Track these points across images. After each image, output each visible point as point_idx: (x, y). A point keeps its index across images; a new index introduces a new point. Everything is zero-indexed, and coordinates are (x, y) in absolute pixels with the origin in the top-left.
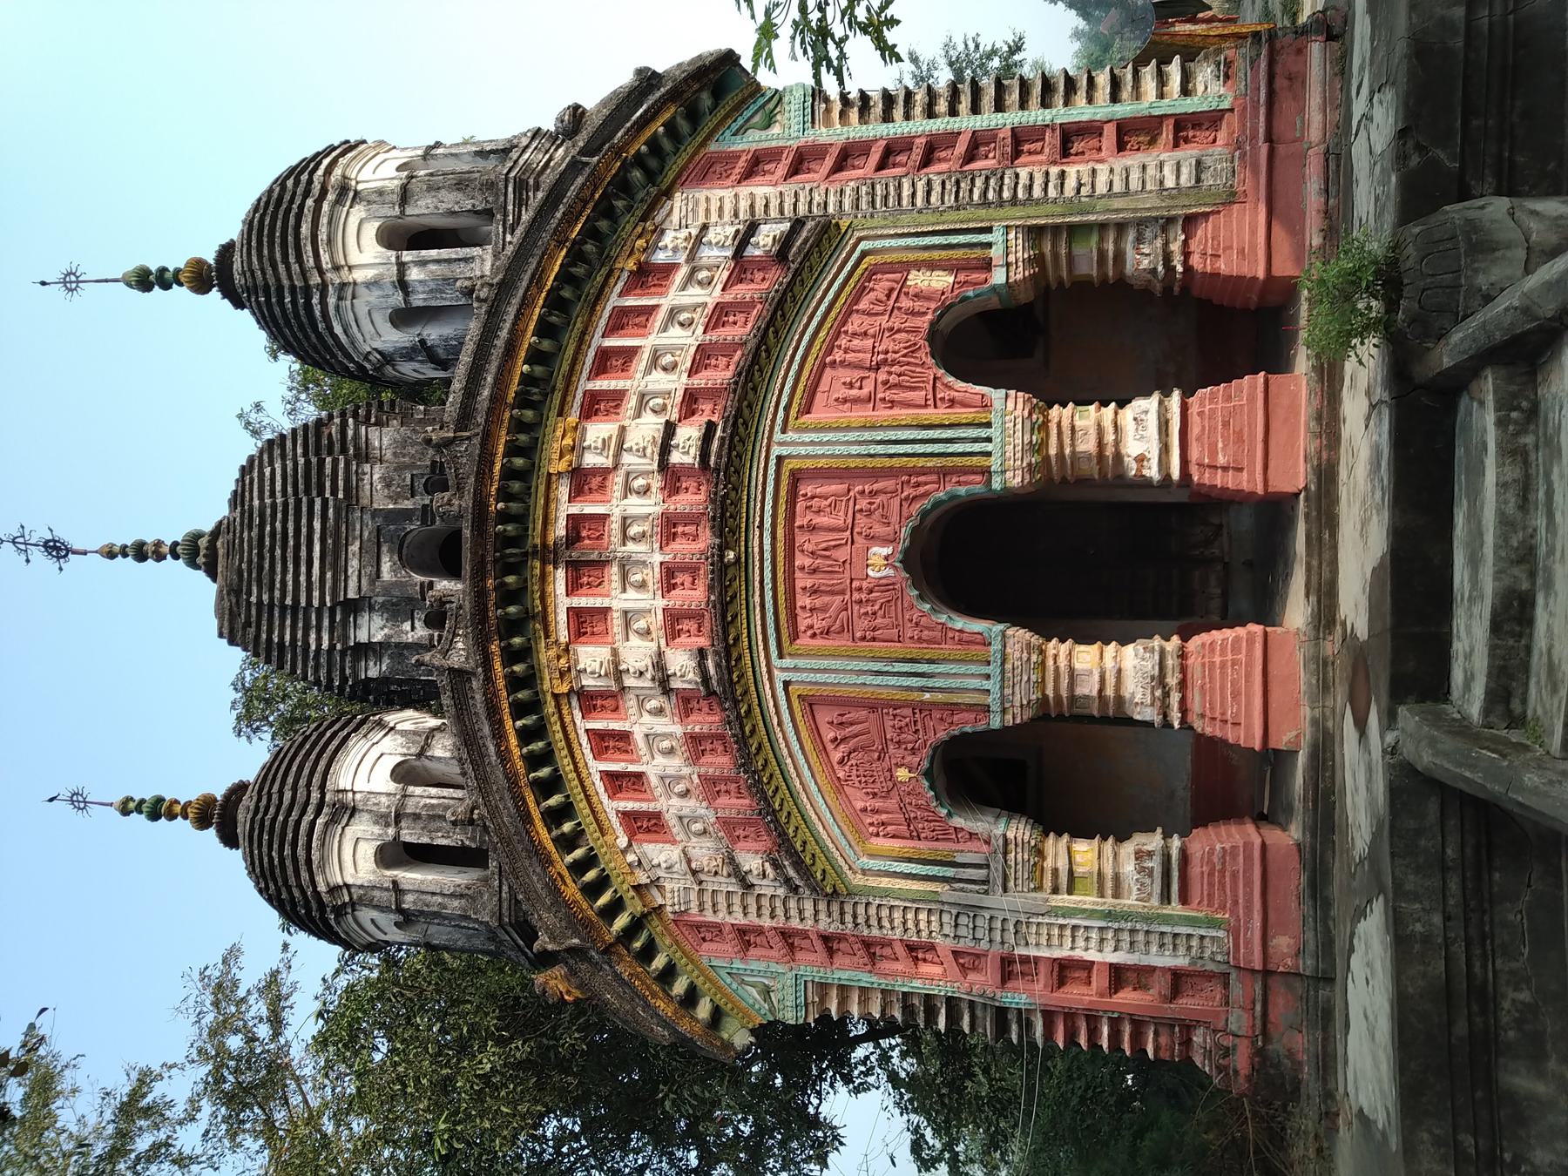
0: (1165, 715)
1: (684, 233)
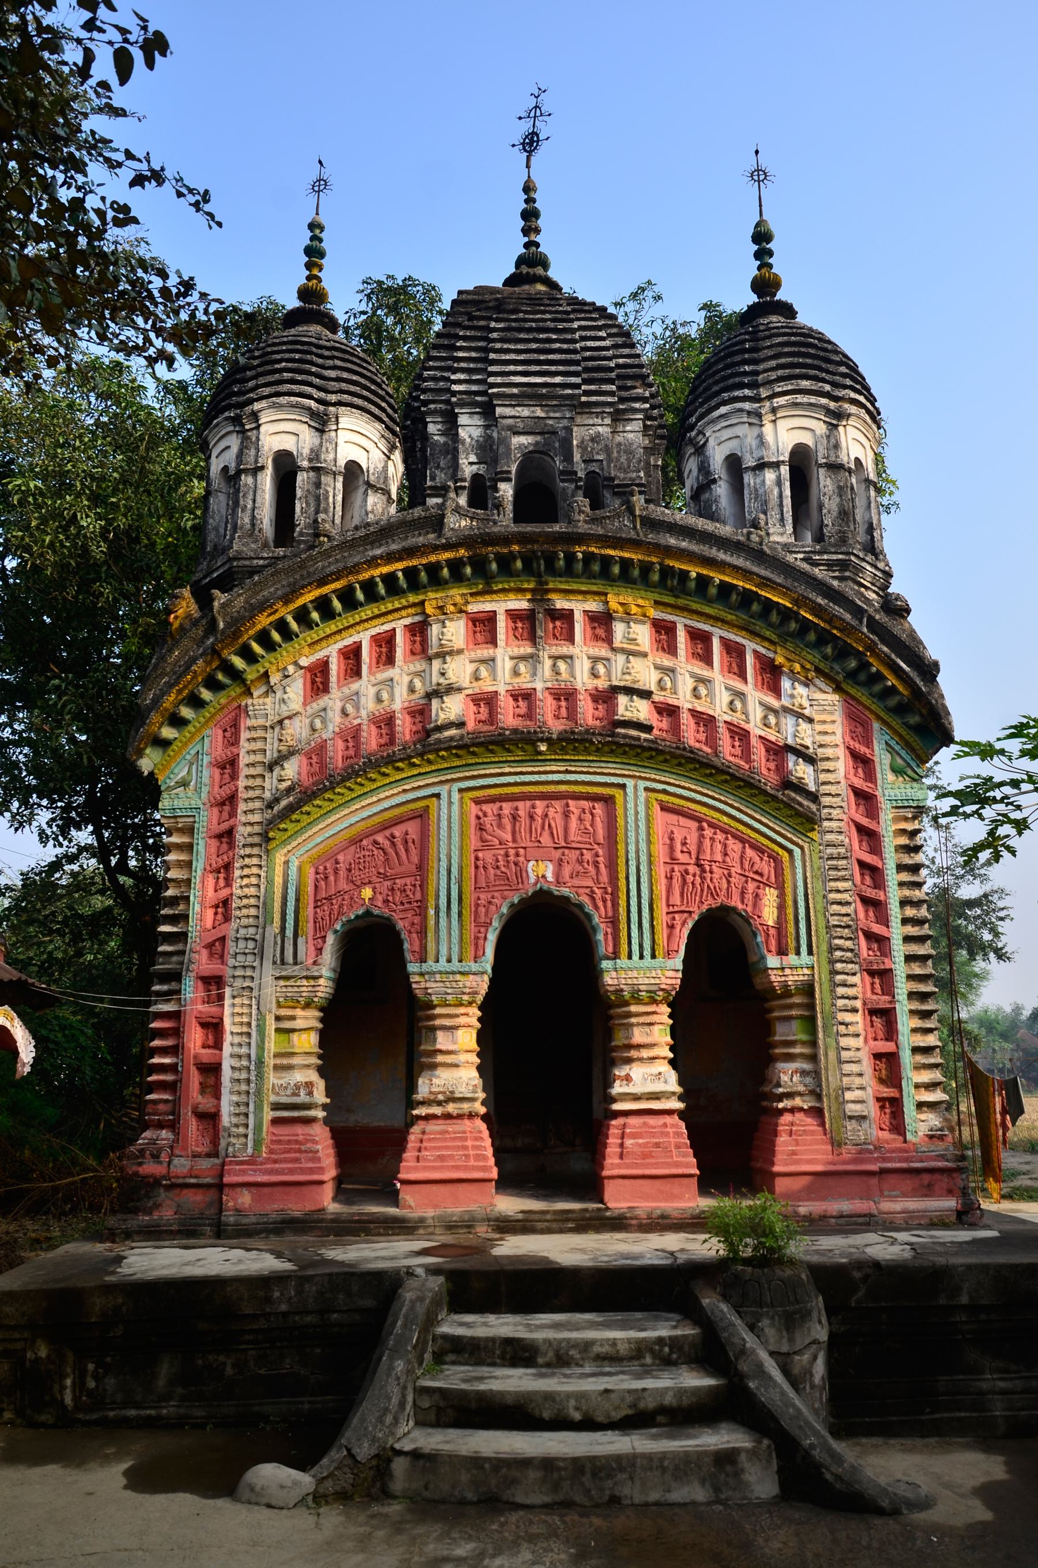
0: (423, 1103)
1: (806, 703)
